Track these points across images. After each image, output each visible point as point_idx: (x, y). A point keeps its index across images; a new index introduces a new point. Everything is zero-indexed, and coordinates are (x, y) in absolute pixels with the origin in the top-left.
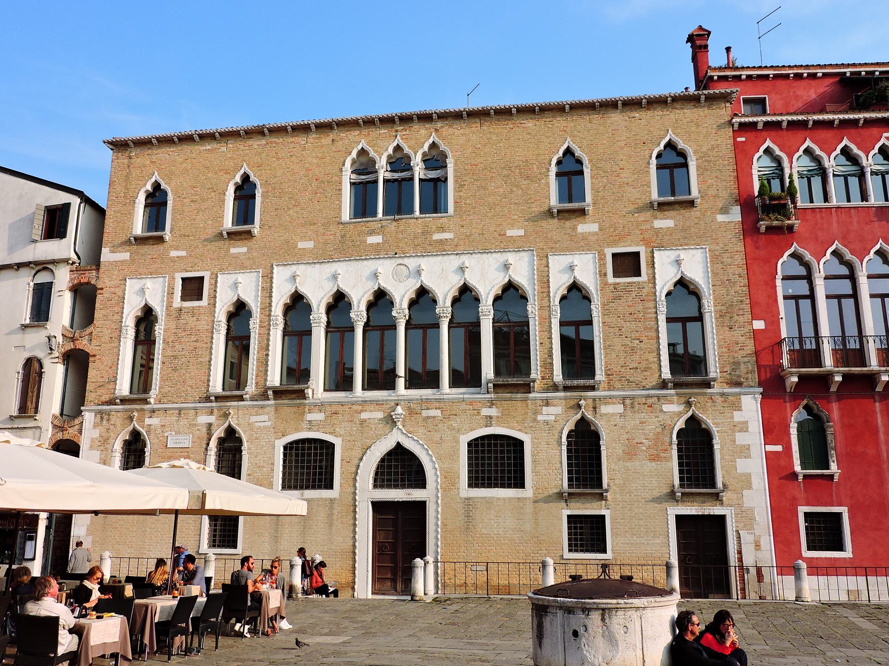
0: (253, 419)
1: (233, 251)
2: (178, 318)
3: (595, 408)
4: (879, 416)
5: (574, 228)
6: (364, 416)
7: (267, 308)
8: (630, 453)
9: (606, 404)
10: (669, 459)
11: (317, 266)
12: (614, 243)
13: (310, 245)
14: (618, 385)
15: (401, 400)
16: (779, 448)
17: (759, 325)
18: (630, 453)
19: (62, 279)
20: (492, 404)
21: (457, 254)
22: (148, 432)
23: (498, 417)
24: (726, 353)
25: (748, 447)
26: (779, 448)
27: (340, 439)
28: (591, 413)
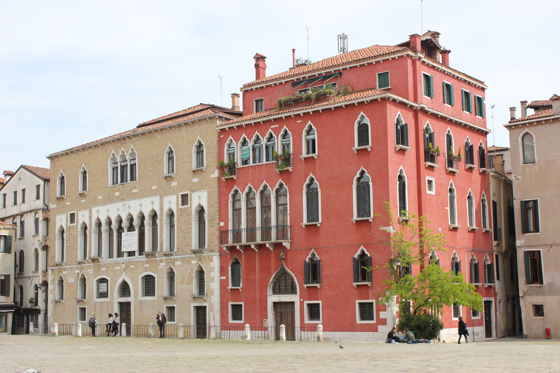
0: (89, 271)
1: (82, 201)
2: (69, 231)
3: (174, 263)
4: (257, 262)
5: (170, 184)
6: (116, 268)
7: (90, 225)
8: (182, 282)
9: (177, 261)
10: (192, 283)
11: (103, 206)
12: (181, 191)
13: (100, 197)
14: (180, 253)
15: (124, 262)
16: (224, 278)
17: (222, 224)
18: (182, 282)
19: (40, 216)
20: (147, 262)
21: (139, 199)
22: (64, 277)
23: (149, 267)
24: (210, 237)
25: (213, 278)
26: (224, 278)
27: (109, 278)
28: (173, 265)
